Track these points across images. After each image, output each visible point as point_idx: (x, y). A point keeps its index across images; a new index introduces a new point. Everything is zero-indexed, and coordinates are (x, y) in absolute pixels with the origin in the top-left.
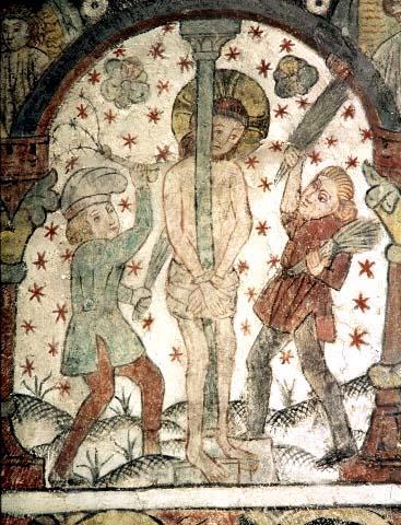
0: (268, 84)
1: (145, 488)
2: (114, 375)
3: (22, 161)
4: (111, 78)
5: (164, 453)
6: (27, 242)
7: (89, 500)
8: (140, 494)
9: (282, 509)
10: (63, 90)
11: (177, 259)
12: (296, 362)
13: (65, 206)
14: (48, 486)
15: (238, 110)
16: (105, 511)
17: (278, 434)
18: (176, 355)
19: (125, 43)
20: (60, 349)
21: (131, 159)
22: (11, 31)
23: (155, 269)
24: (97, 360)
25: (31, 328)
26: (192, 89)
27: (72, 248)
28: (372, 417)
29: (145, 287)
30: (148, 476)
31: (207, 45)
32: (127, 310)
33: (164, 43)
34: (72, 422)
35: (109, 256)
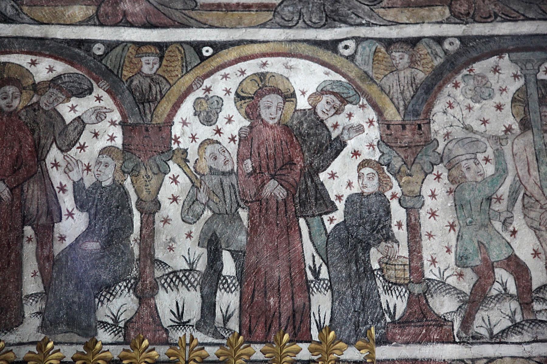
1: (529, 343)
2: (493, 267)
3: (413, 134)
4: (467, 85)
5: (539, 319)
6: (422, 183)
7: (490, 350)
8: (527, 347)
10: (436, 93)
11: (527, 193)
13: (445, 162)
14: (457, 340)
16: (502, 358)
18: (536, 254)
19: (474, 65)
20: (453, 250)
21: (487, 133)
22: (397, 59)
23: (513, 200)
24: (480, 258)
25: (432, 236)
26: (523, 91)
27: (453, 187)
29: (508, 211)
30: (529, 334)
31: (529, 66)
32: (498, 225)
33: (500, 65)
34: (467, 297)
35: (480, 191)
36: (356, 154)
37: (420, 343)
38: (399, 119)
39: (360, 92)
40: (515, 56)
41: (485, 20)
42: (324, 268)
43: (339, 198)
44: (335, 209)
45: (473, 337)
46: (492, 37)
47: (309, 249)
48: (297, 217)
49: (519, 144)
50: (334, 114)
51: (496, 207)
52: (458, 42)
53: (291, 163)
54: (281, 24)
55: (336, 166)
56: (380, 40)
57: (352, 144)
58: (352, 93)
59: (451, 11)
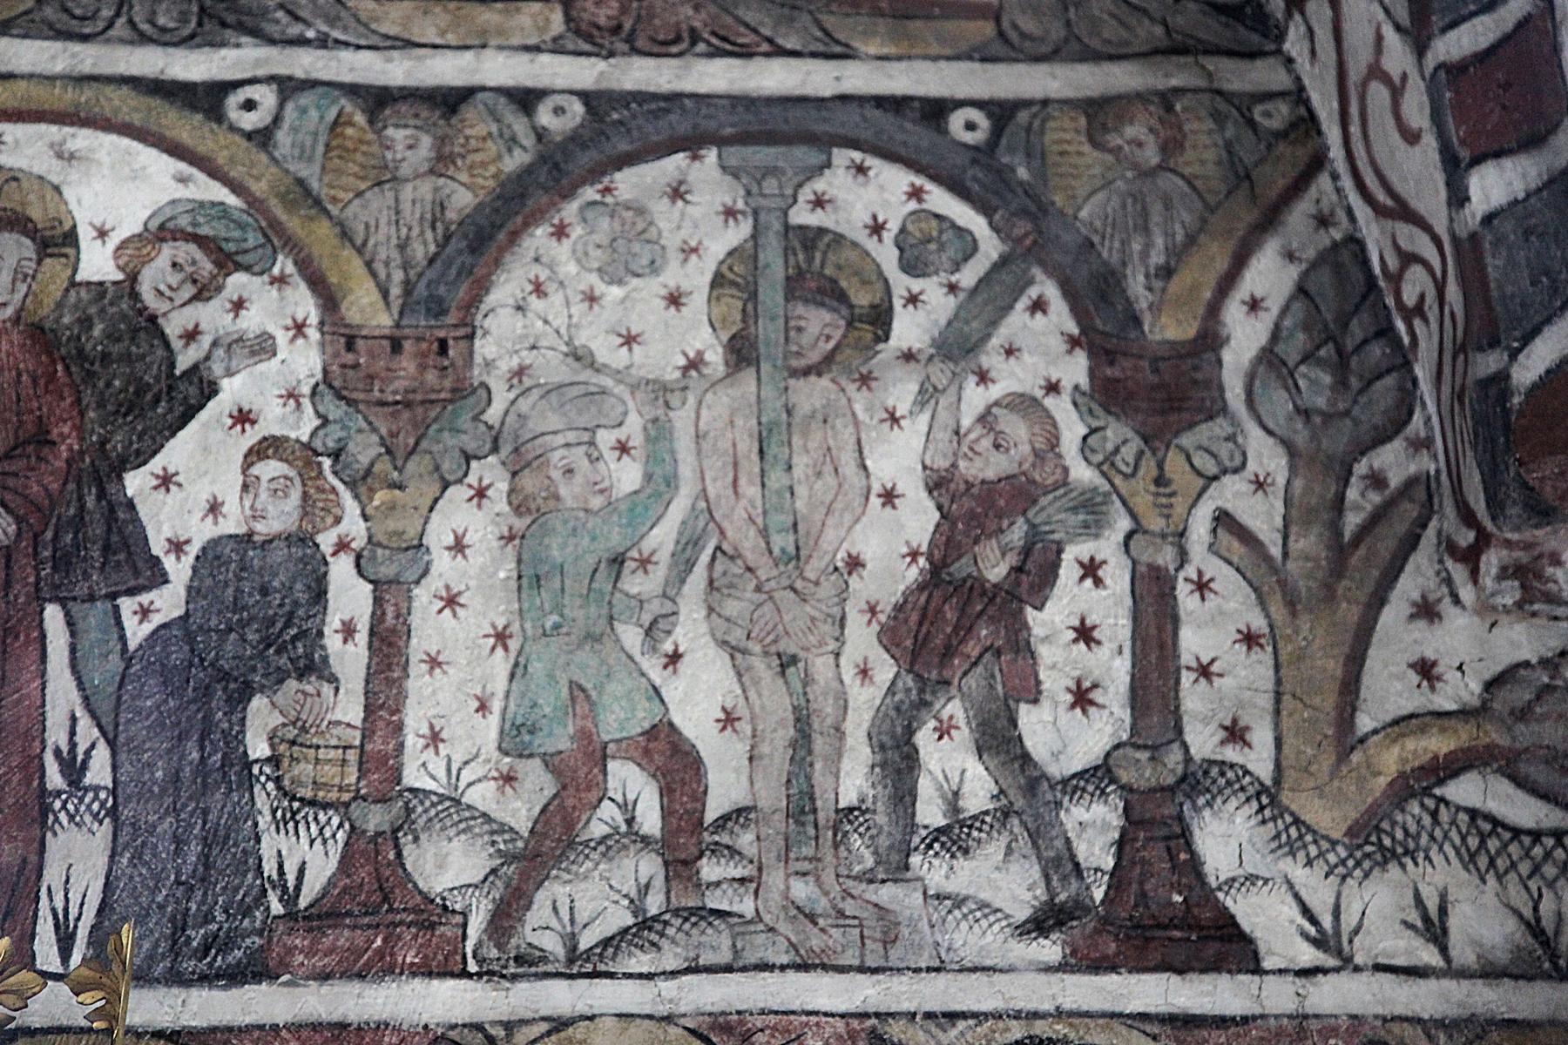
0: (886, 255)
1: (674, 974)
2: (605, 757)
3: (423, 368)
4: (592, 232)
5: (711, 905)
6: (431, 509)
7: (560, 997)
8: (667, 987)
9: (953, 1016)
10: (502, 250)
11: (725, 546)
12: (963, 734)
13: (506, 450)
14: (472, 967)
15: (832, 295)
16: (591, 1018)
17: (935, 871)
18: (728, 720)
19: (618, 176)
20: (496, 705)
21: (633, 371)
22: (400, 147)
23: (683, 565)
24: (571, 730)
25: (439, 664)
27: (520, 524)
28: (1121, 844)
29: (664, 595)
30: (679, 950)
31: (770, 185)
32: (631, 636)
33: (690, 179)
34: (520, 844)
35: (594, 539)
36: (243, 418)
37: (361, 976)
38: (384, 320)
39: (276, 237)
40: (735, 155)
41: (665, 46)
42: (102, 754)
43: (177, 547)
44: (162, 579)
45: (519, 960)
46: (675, 97)
47: (62, 693)
48: (40, 601)
49: (719, 405)
50: (190, 301)
51: (634, 583)
52: (577, 108)
53: (42, 439)
54: (58, 26)
55: (178, 452)
56: (352, 90)
57: (233, 390)
58: (253, 239)
59: (568, 19)
